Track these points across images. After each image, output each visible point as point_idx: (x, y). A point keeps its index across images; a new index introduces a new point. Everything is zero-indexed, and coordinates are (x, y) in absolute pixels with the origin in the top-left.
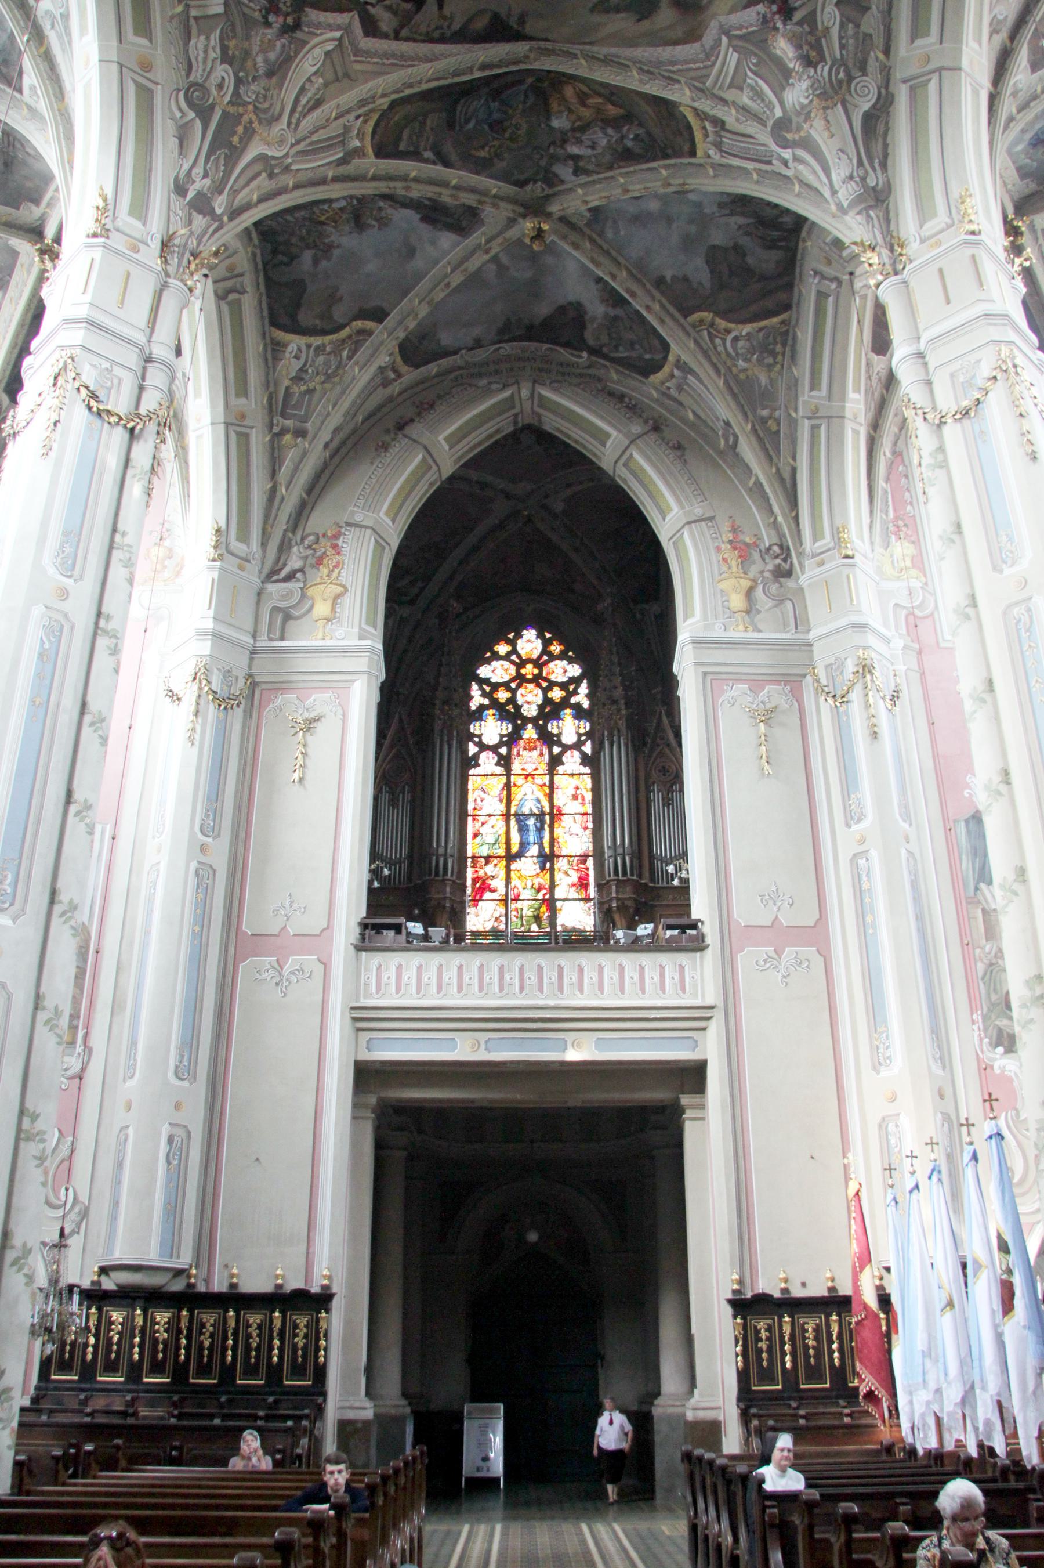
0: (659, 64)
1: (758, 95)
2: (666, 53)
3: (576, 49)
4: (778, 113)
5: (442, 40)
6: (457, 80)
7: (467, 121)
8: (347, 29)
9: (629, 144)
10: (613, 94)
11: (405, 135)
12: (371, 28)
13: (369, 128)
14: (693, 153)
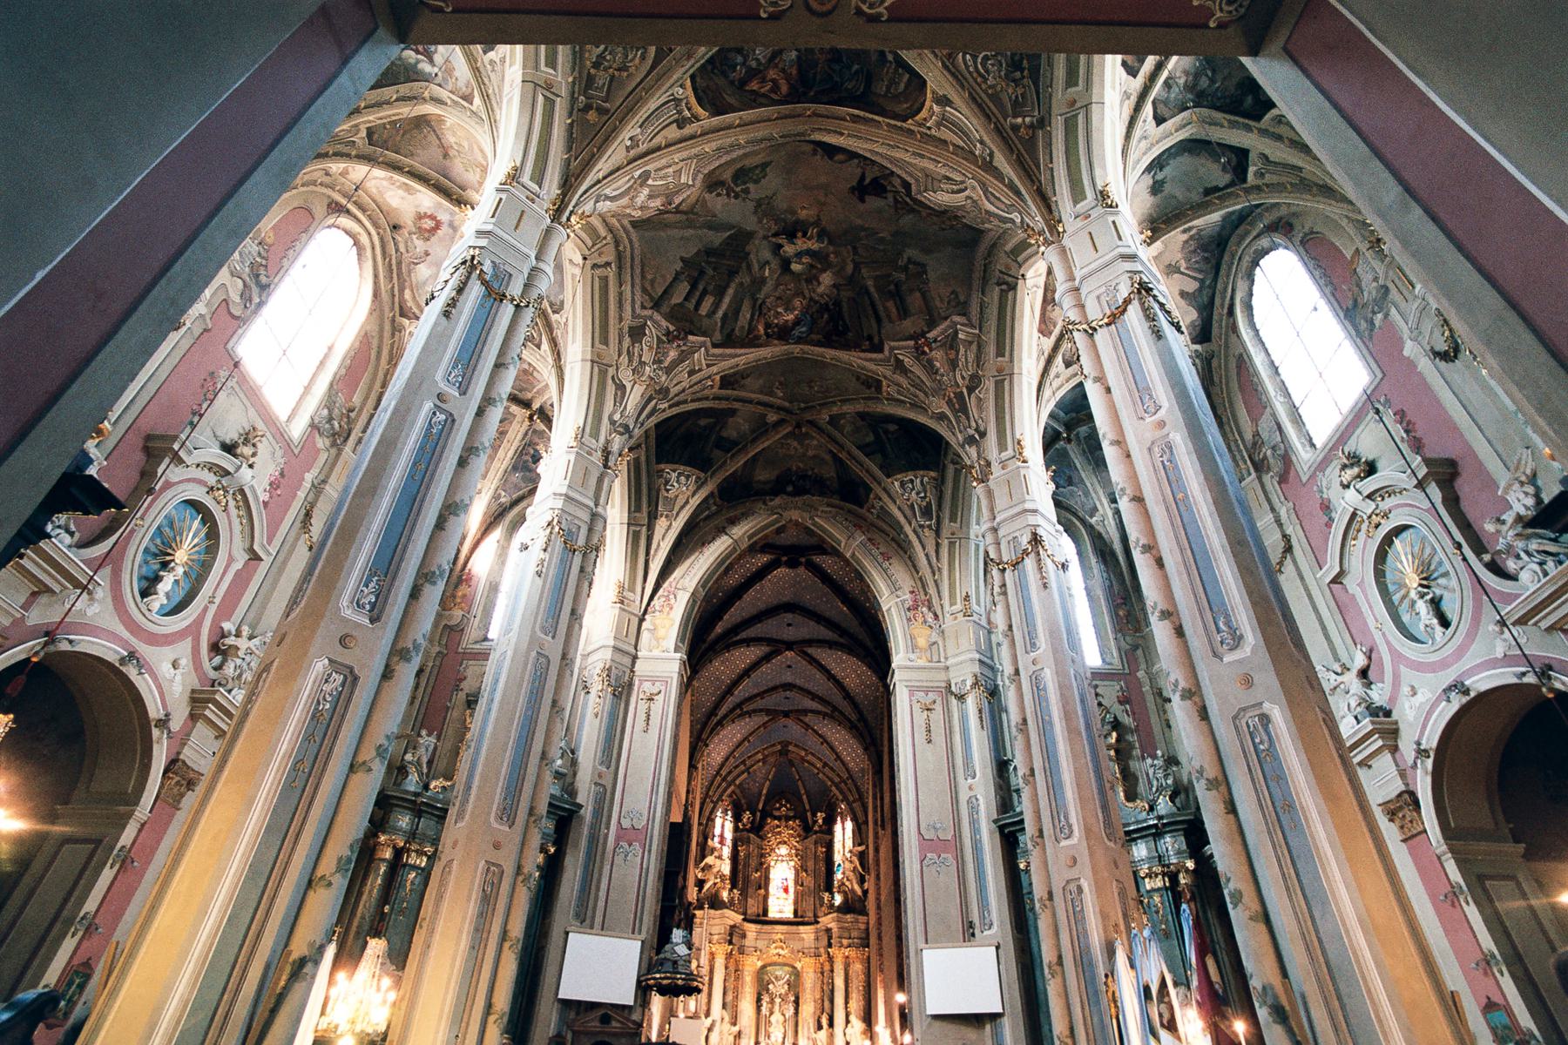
0: (727, 153)
1: (661, 178)
2: (723, 160)
3: (781, 141)
4: (650, 182)
5: (866, 158)
6: (862, 113)
7: (857, 72)
8: (920, 192)
9: (740, 59)
10: (754, 100)
11: (902, 86)
12: (907, 185)
13: (924, 114)
14: (693, 77)
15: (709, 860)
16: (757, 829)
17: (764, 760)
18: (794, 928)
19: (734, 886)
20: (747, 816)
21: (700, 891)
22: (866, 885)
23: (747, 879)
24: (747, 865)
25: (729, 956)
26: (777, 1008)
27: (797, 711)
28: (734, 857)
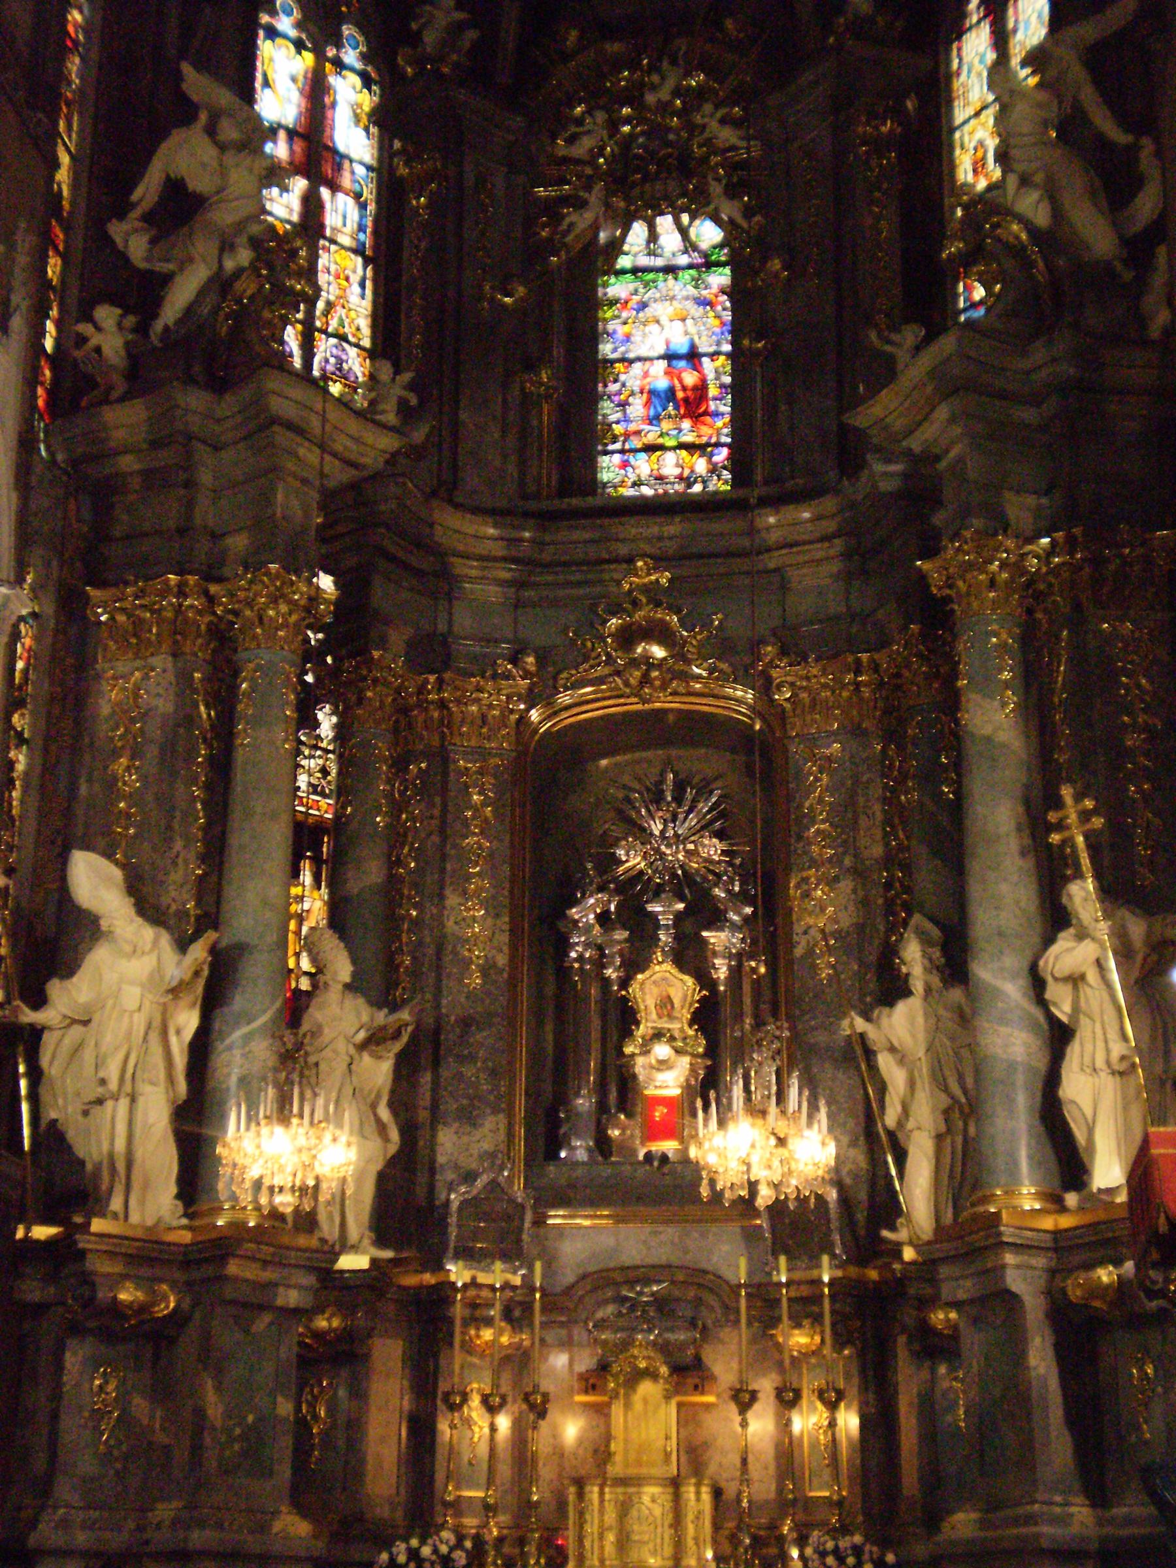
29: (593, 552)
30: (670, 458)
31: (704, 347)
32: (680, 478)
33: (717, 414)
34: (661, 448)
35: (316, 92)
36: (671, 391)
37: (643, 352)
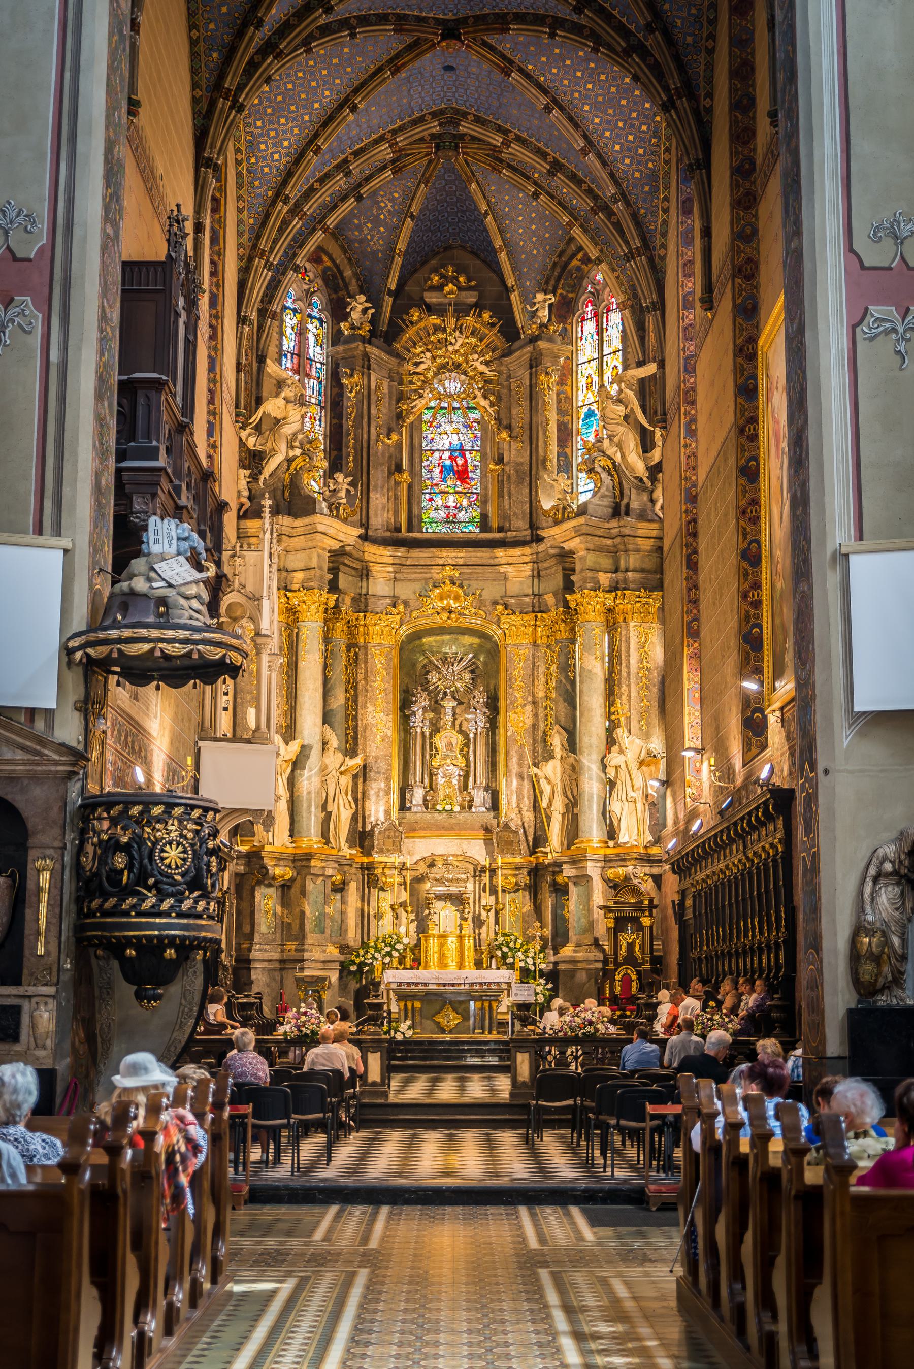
15: (273, 407)
16: (387, 334)
17: (397, 165)
18: (483, 555)
19: (335, 466)
20: (358, 307)
21: (254, 477)
22: (656, 455)
23: (365, 452)
24: (363, 418)
25: (332, 614)
26: (447, 717)
27: (480, 19)
28: (335, 404)
29: (428, 562)
30: (451, 498)
31: (467, 446)
32: (455, 507)
33: (472, 479)
34: (447, 493)
35: (301, 332)
36: (452, 466)
37: (440, 447)
